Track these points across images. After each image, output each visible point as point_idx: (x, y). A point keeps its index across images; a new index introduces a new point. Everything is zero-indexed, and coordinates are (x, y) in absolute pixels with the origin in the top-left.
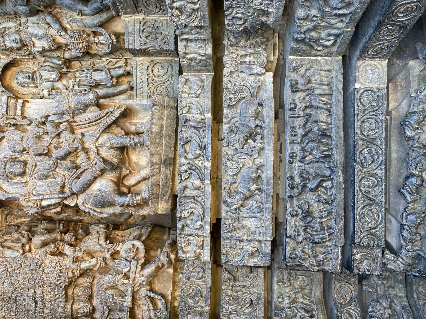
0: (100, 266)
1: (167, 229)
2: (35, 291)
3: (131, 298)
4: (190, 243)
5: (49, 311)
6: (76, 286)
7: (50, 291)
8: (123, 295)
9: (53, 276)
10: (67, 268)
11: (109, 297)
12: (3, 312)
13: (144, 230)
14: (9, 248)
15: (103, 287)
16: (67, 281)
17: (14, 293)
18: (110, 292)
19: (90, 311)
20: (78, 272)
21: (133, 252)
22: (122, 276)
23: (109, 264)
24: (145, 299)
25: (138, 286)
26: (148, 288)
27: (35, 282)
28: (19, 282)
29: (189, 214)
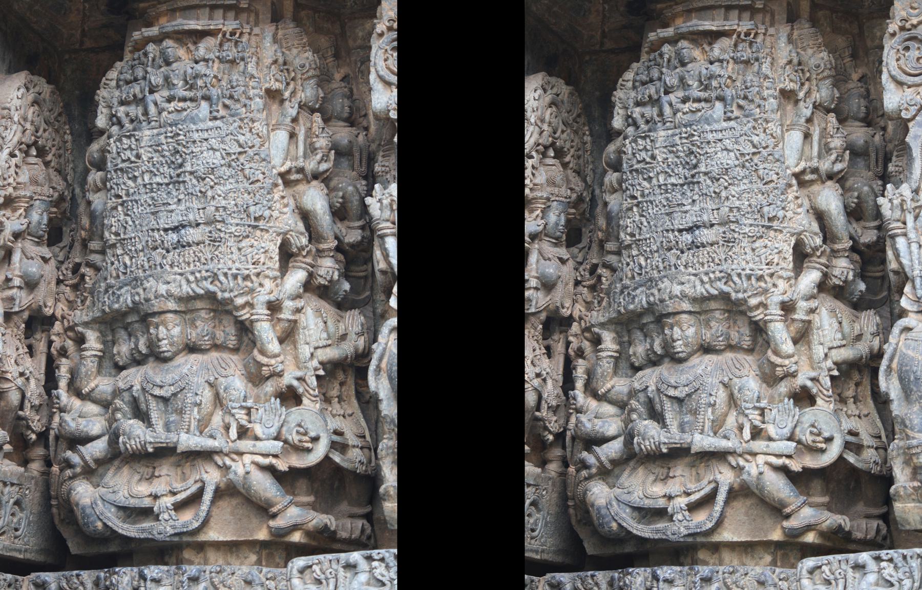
0: (777, 366)
1: (884, 510)
4: (830, 584)
6: (729, 311)
7: (717, 261)
8: (717, 427)
12: (664, 156)
13: (870, 455)
14: (807, 136)
15: (731, 377)
16: (740, 296)
17: (706, 178)
18: (721, 396)
22: (757, 423)
23: (783, 384)
25: (738, 464)
26: (736, 486)
27: (733, 222)
29: (888, 578)
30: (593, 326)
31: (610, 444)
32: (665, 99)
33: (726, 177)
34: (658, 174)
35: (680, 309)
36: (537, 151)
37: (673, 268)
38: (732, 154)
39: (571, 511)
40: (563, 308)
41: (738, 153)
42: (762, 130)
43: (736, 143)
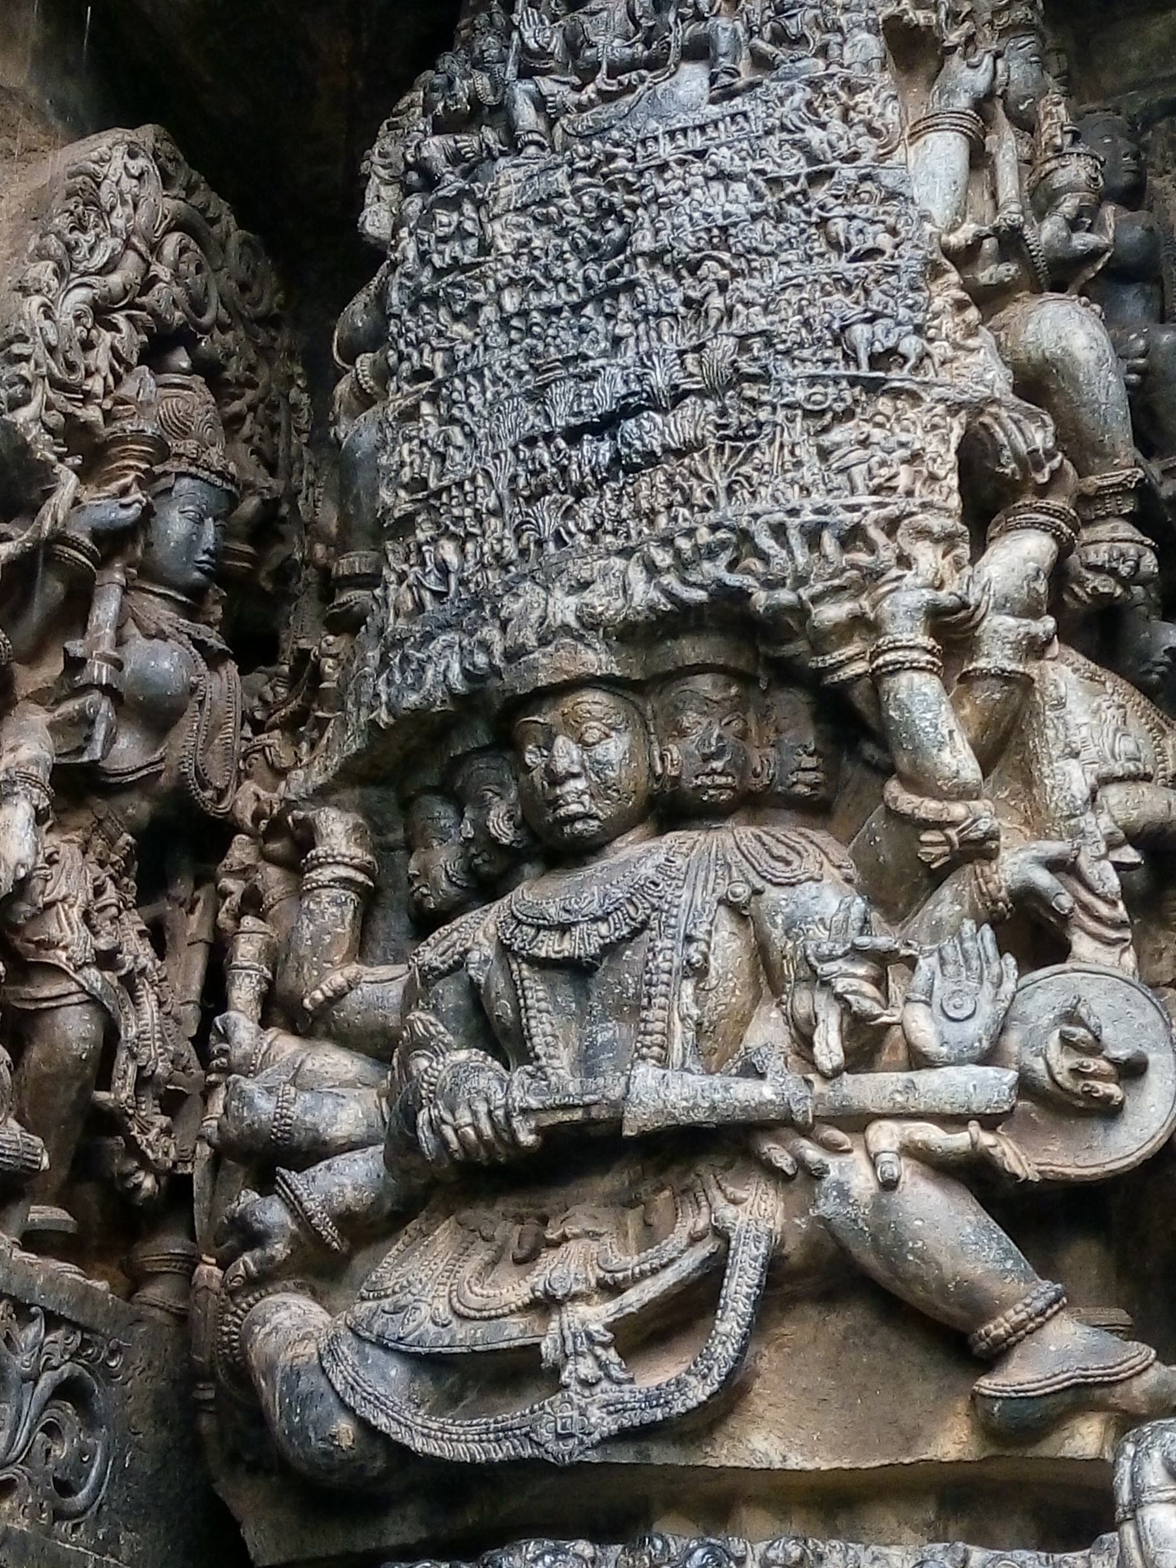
2: (687, 393)
3: (699, 1116)
5: (548, 532)
6: (745, 679)
7: (699, 497)
9: (806, 490)
10: (873, 576)
11: (689, 939)
12: (520, 235)
15: (759, 884)
16: (785, 596)
19: (573, 819)
20: (860, 667)
21: (1077, 1073)
23: (946, 892)
24: (694, 1240)
25: (800, 1162)
27: (752, 378)
28: (735, 274)
30: (289, 805)
31: (338, 1161)
32: (521, 91)
33: (726, 256)
34: (499, 288)
35: (576, 669)
36: (129, 318)
37: (551, 547)
38: (741, 188)
39: (206, 1423)
40: (204, 787)
41: (760, 182)
42: (836, 111)
43: (756, 153)
